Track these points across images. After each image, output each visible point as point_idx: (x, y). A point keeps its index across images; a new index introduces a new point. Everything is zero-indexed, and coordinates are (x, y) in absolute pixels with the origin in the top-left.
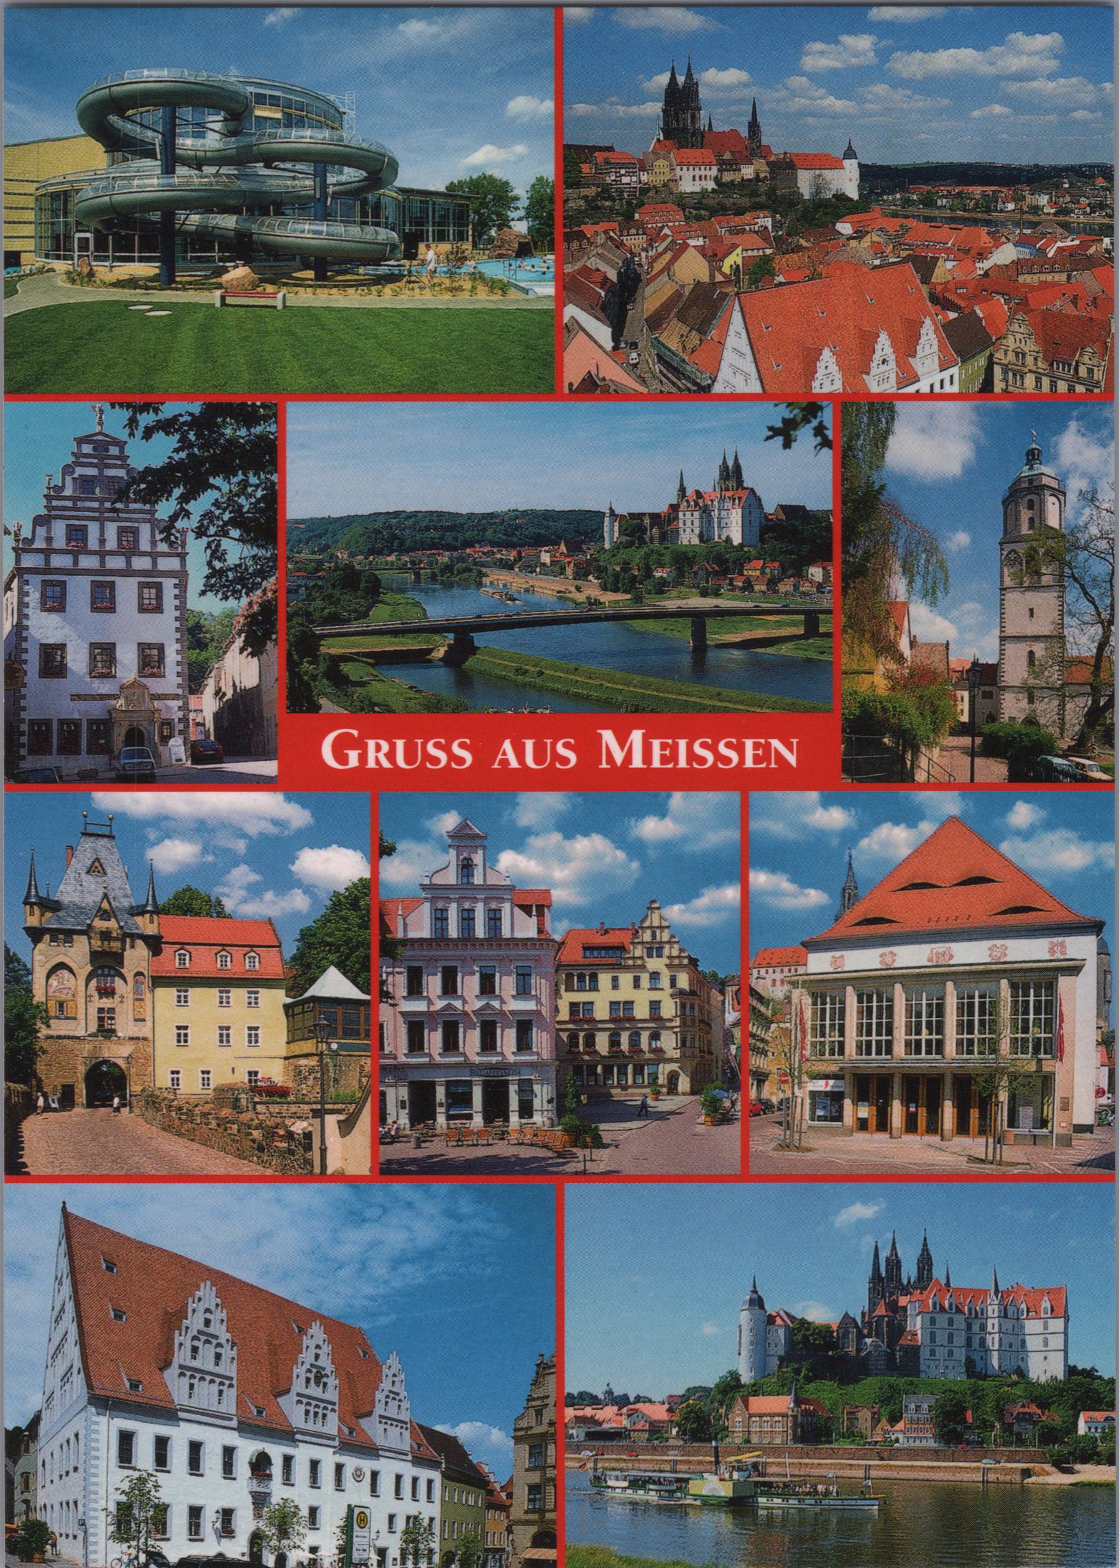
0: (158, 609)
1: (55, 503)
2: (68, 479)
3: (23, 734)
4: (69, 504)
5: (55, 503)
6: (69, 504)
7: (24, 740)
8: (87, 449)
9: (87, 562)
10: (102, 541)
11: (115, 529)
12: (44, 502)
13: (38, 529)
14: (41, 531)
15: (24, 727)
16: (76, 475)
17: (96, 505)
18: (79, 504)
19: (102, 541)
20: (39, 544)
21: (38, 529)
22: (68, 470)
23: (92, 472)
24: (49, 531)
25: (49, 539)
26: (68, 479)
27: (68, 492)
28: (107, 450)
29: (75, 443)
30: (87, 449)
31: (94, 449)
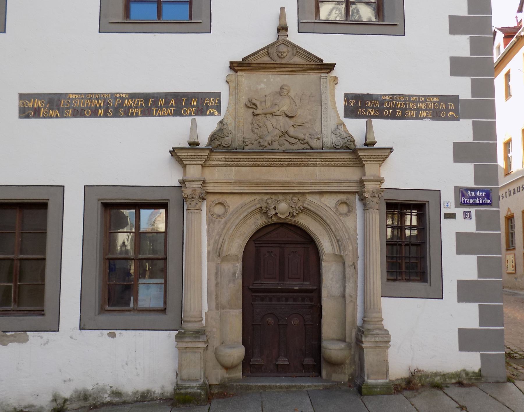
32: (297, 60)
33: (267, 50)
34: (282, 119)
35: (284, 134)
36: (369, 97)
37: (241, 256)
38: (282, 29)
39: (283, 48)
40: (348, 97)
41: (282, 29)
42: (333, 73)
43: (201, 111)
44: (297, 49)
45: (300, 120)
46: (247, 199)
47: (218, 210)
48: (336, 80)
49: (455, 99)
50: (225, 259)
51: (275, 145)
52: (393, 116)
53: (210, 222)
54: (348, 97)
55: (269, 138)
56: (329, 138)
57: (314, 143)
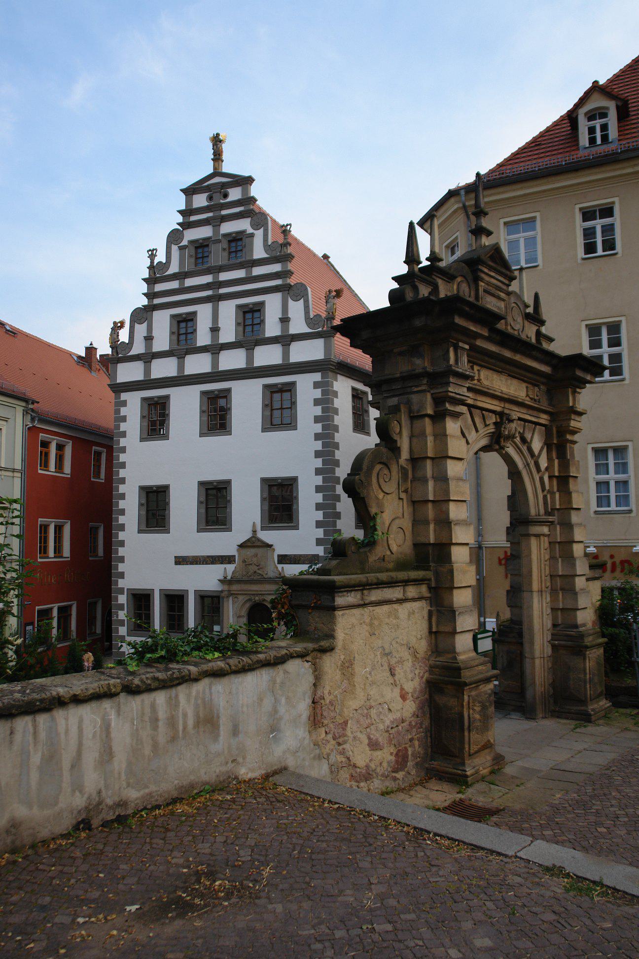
0: (290, 424)
1: (159, 287)
2: (175, 248)
3: (121, 607)
4: (174, 285)
5: (159, 287)
6: (174, 285)
7: (122, 615)
8: (201, 201)
9: (198, 364)
10: (215, 330)
11: (233, 310)
12: (144, 288)
13: (137, 326)
14: (141, 330)
15: (122, 599)
16: (184, 243)
17: (207, 279)
18: (189, 282)
19: (215, 330)
20: (138, 348)
21: (137, 326)
22: (174, 237)
23: (205, 232)
24: (150, 329)
25: (149, 339)
26: (175, 248)
27: (174, 268)
28: (226, 196)
29: (183, 196)
30: (201, 201)
31: (210, 198)
32: (259, 544)
33: (248, 540)
34: (255, 567)
35: (255, 572)
36: (286, 556)
37: (245, 615)
38: (254, 532)
39: (253, 539)
40: (279, 556)
41: (254, 532)
42: (273, 547)
43: (230, 563)
44: (259, 540)
45: (261, 566)
46: (244, 596)
47: (236, 599)
48: (274, 550)
49: (318, 555)
50: (239, 617)
51: (252, 577)
52: (295, 563)
53: (233, 604)
54: (279, 556)
55: (249, 574)
56: (271, 574)
57: (264, 576)
